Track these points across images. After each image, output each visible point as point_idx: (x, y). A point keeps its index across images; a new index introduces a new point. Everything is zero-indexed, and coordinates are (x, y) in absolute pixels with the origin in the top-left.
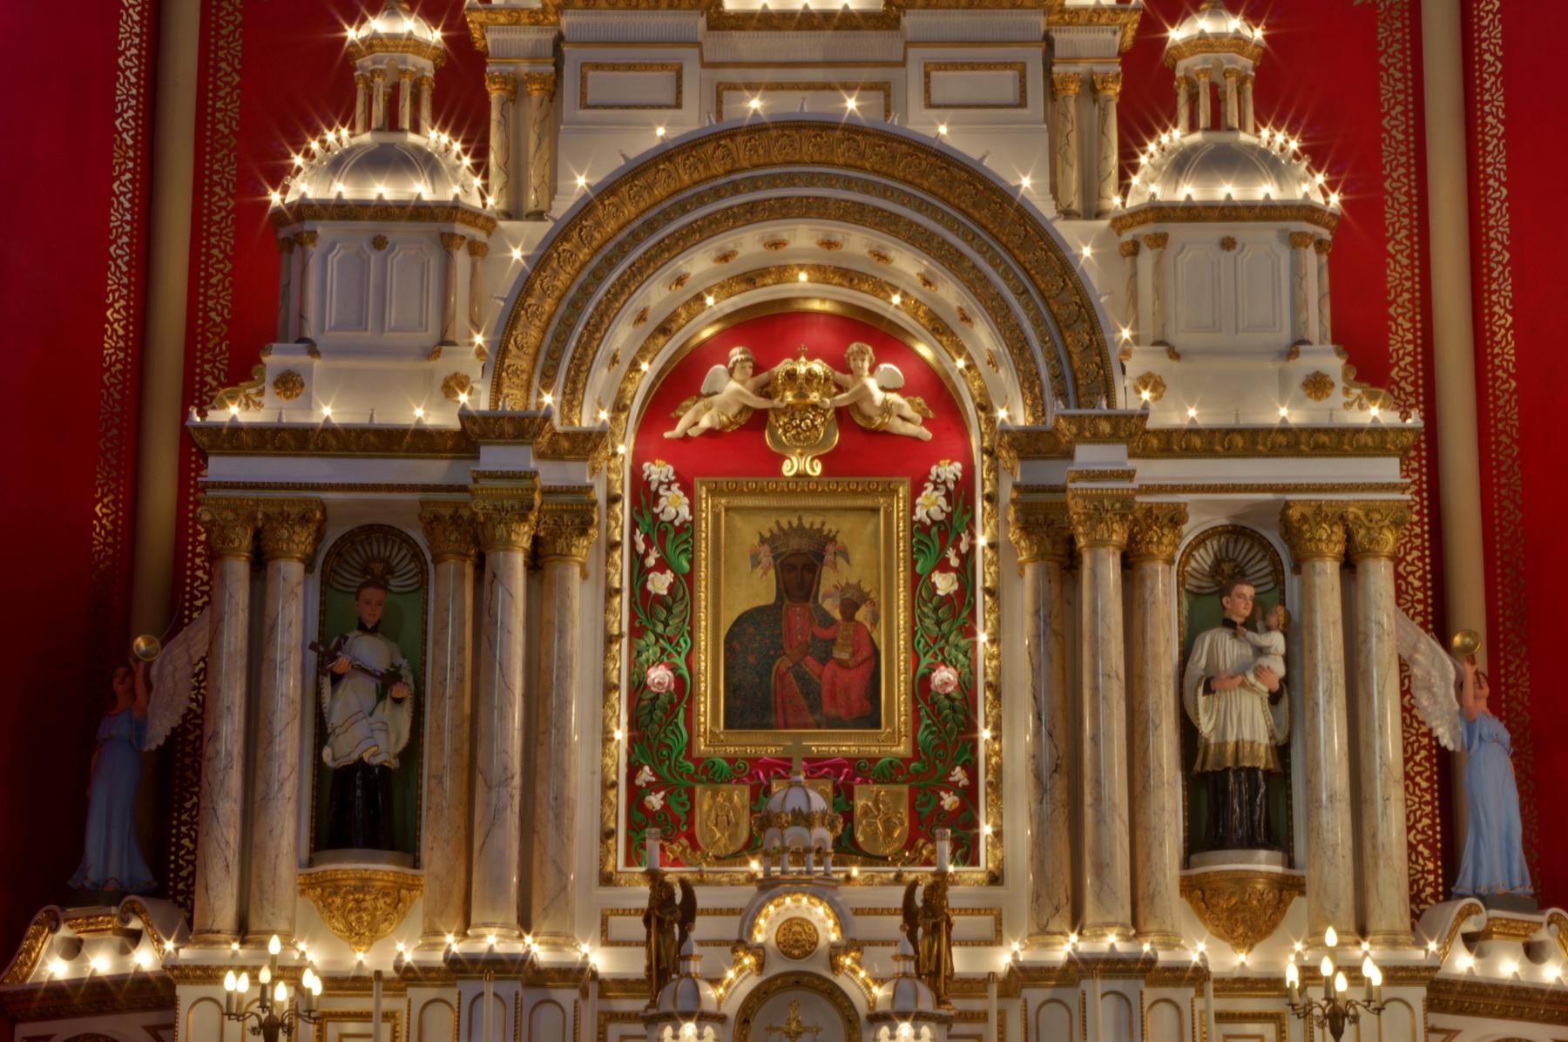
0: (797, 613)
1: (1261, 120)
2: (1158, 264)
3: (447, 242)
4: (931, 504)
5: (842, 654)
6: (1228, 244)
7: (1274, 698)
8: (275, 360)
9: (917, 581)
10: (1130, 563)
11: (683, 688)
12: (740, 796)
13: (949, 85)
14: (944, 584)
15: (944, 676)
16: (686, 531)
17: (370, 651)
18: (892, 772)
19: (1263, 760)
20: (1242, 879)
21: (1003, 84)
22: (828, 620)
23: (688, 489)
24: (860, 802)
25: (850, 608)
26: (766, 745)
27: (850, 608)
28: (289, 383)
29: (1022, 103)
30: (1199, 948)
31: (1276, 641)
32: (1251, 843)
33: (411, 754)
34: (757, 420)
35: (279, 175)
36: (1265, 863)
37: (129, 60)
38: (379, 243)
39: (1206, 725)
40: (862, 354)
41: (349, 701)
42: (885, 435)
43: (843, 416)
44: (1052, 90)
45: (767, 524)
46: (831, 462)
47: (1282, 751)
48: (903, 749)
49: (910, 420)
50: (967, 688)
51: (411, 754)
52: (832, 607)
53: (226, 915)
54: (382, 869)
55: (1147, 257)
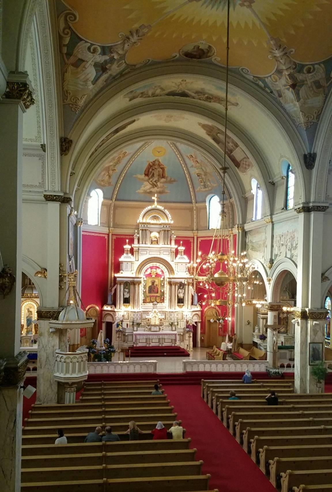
0: (153, 286)
1: (184, 255)
2: (178, 266)
3: (132, 263)
4: (162, 279)
5: (156, 289)
6: (182, 264)
7: (183, 294)
8: (121, 271)
9: (161, 284)
10: (175, 286)
11: (146, 291)
12: (149, 298)
13: (164, 253)
14: (163, 284)
15: (162, 291)
16: (146, 280)
17: (127, 290)
18: (159, 297)
19: (182, 298)
20: (180, 305)
21: (168, 253)
22: (155, 286)
23: (146, 278)
24: (157, 299)
25: (156, 286)
26: (152, 295)
27: (156, 286)
28: (122, 273)
29: (169, 254)
30: (178, 309)
31: (183, 290)
32: (181, 303)
33: (129, 297)
34: (151, 273)
35: (120, 257)
36: (182, 304)
37: (107, 244)
38: (127, 263)
39: (179, 295)
40: (157, 269)
41: (125, 294)
42: (159, 274)
43: (156, 273)
44: (171, 252)
45: (151, 280)
46: (156, 276)
47: (183, 297)
48: (159, 295)
49: (160, 273)
50: (164, 291)
51: (129, 297)
52: (155, 285)
53: (119, 308)
54: (128, 304)
55: (177, 265)
